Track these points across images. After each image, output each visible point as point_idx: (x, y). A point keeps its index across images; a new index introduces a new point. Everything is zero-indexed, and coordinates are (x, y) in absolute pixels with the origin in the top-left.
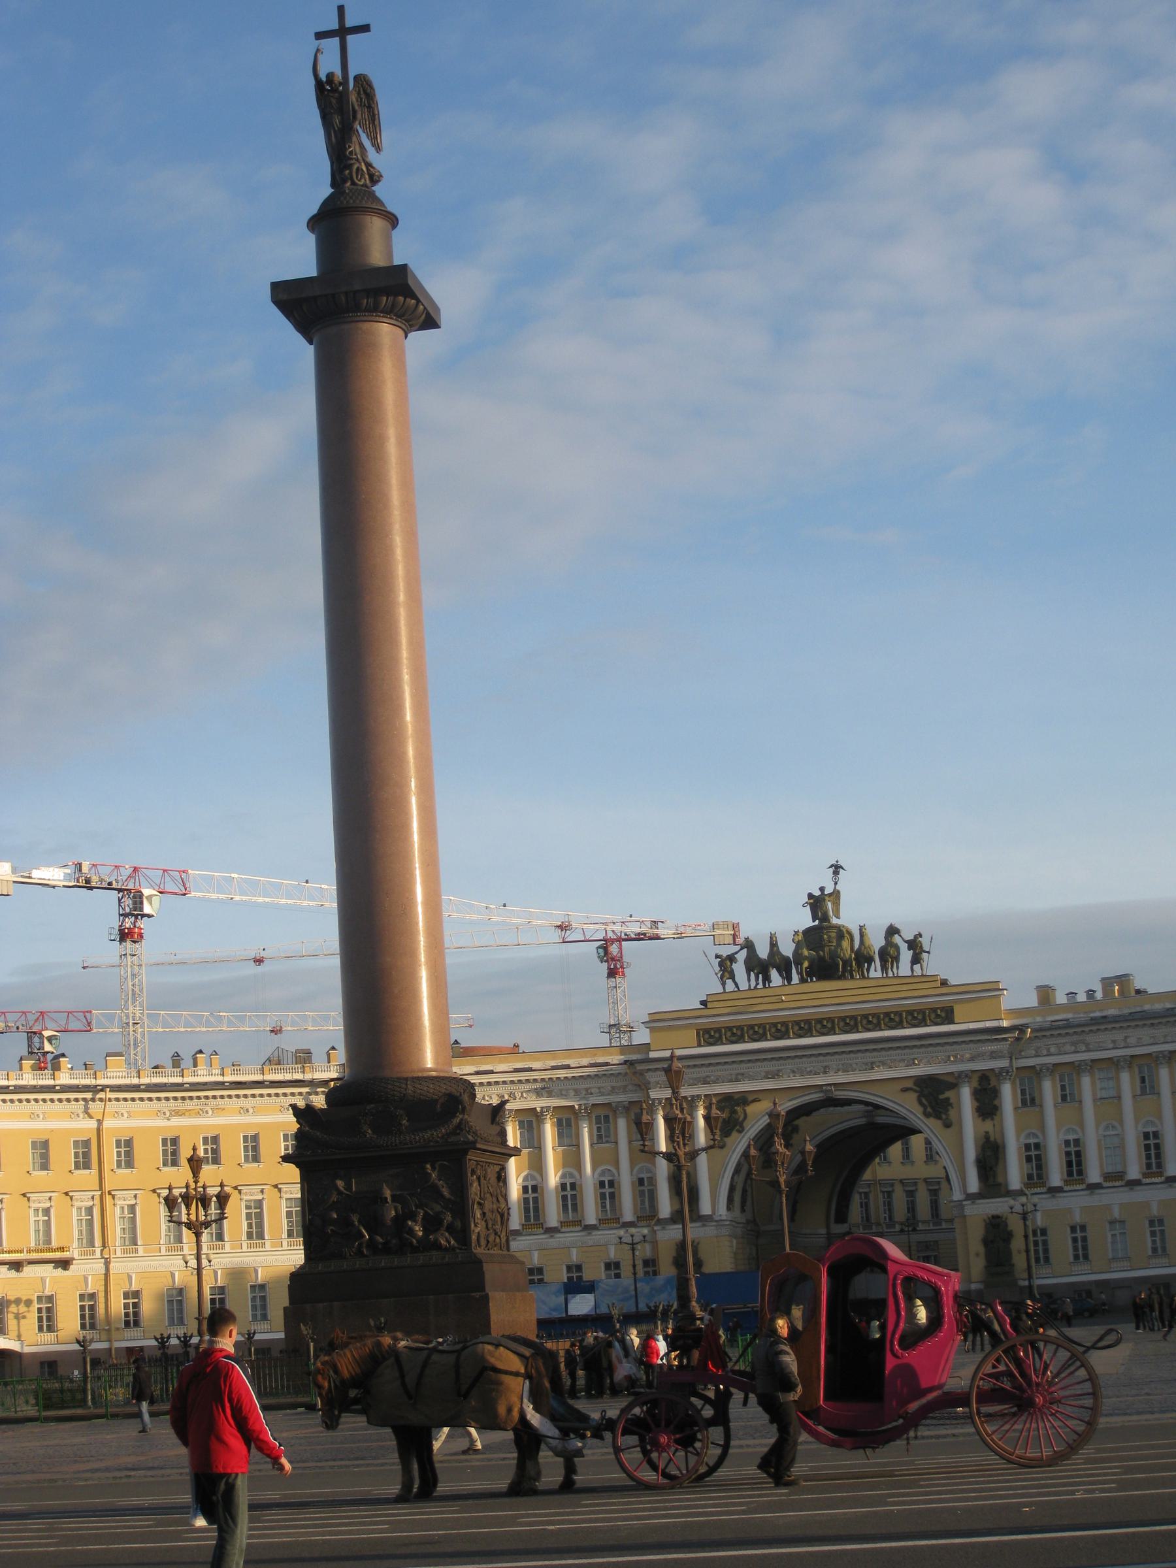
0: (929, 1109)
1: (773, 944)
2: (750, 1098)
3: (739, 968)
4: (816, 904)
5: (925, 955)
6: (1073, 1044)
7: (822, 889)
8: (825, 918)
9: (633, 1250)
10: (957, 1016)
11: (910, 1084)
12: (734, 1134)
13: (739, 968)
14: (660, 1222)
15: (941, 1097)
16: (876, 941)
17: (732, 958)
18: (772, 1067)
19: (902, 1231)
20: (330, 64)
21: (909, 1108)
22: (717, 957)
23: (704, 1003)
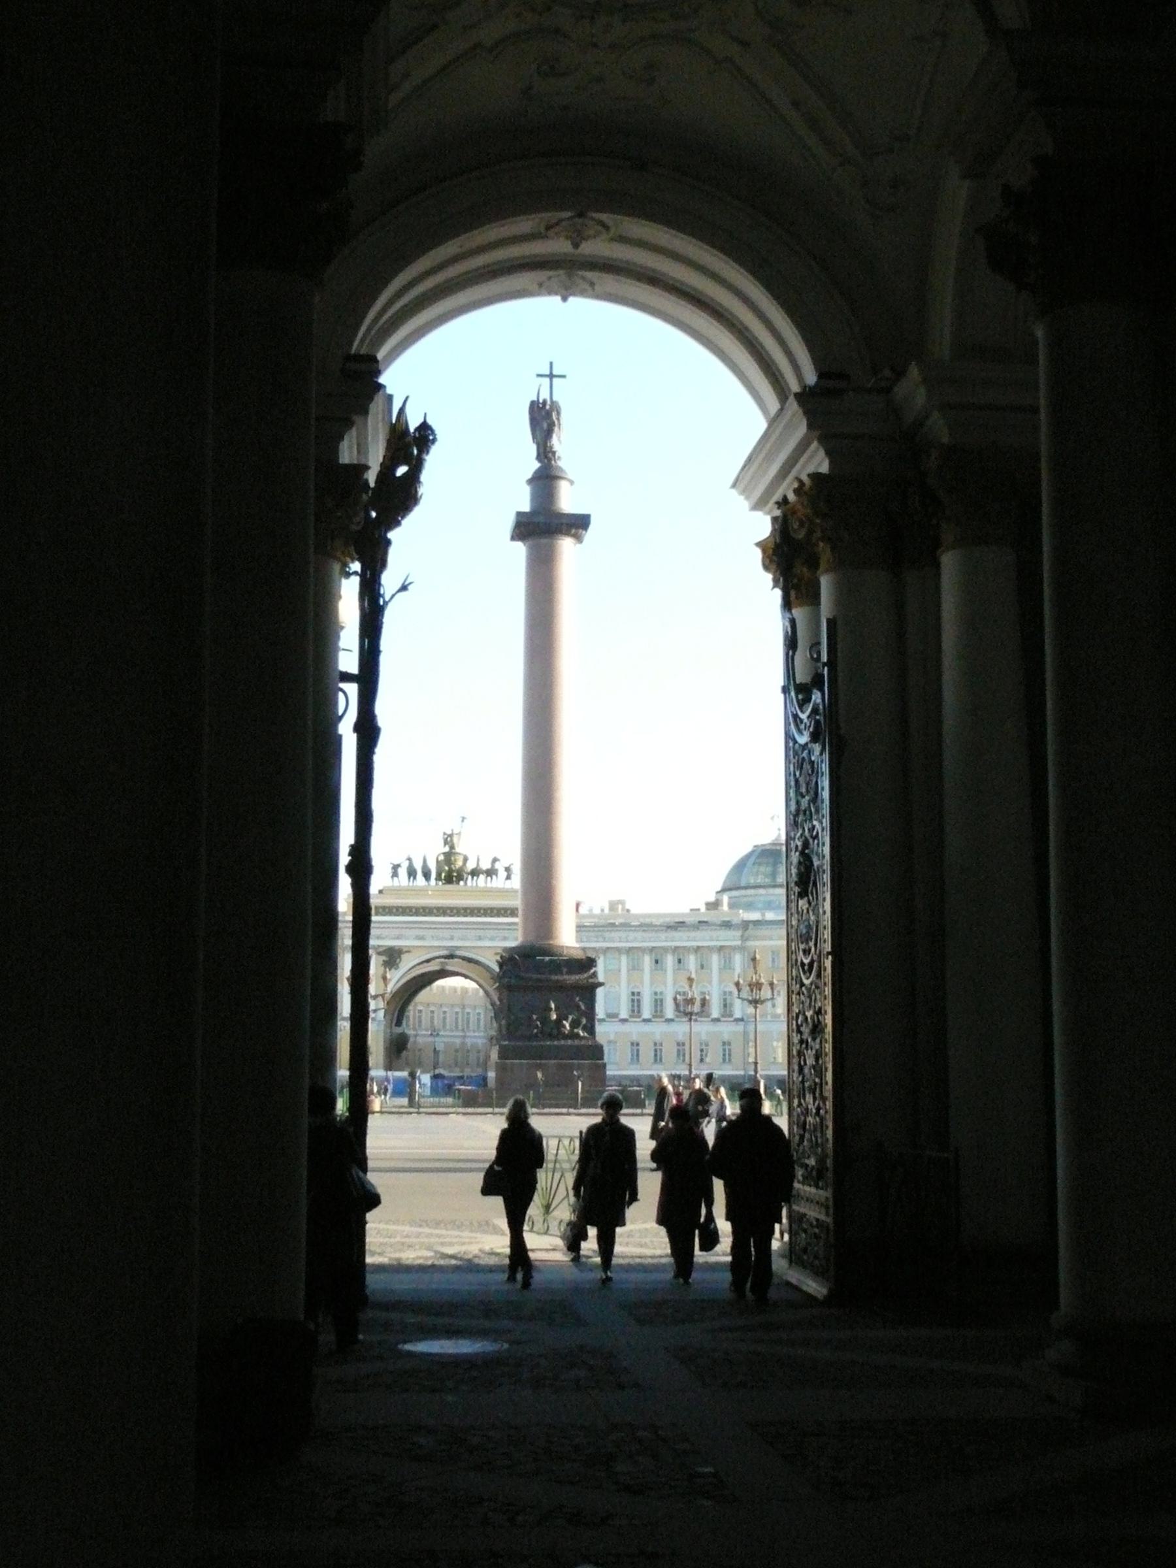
1: (425, 861)
3: (403, 872)
4: (448, 840)
6: (597, 937)
8: (452, 847)
13: (403, 872)
16: (485, 865)
17: (399, 866)
18: (421, 933)
20: (544, 395)
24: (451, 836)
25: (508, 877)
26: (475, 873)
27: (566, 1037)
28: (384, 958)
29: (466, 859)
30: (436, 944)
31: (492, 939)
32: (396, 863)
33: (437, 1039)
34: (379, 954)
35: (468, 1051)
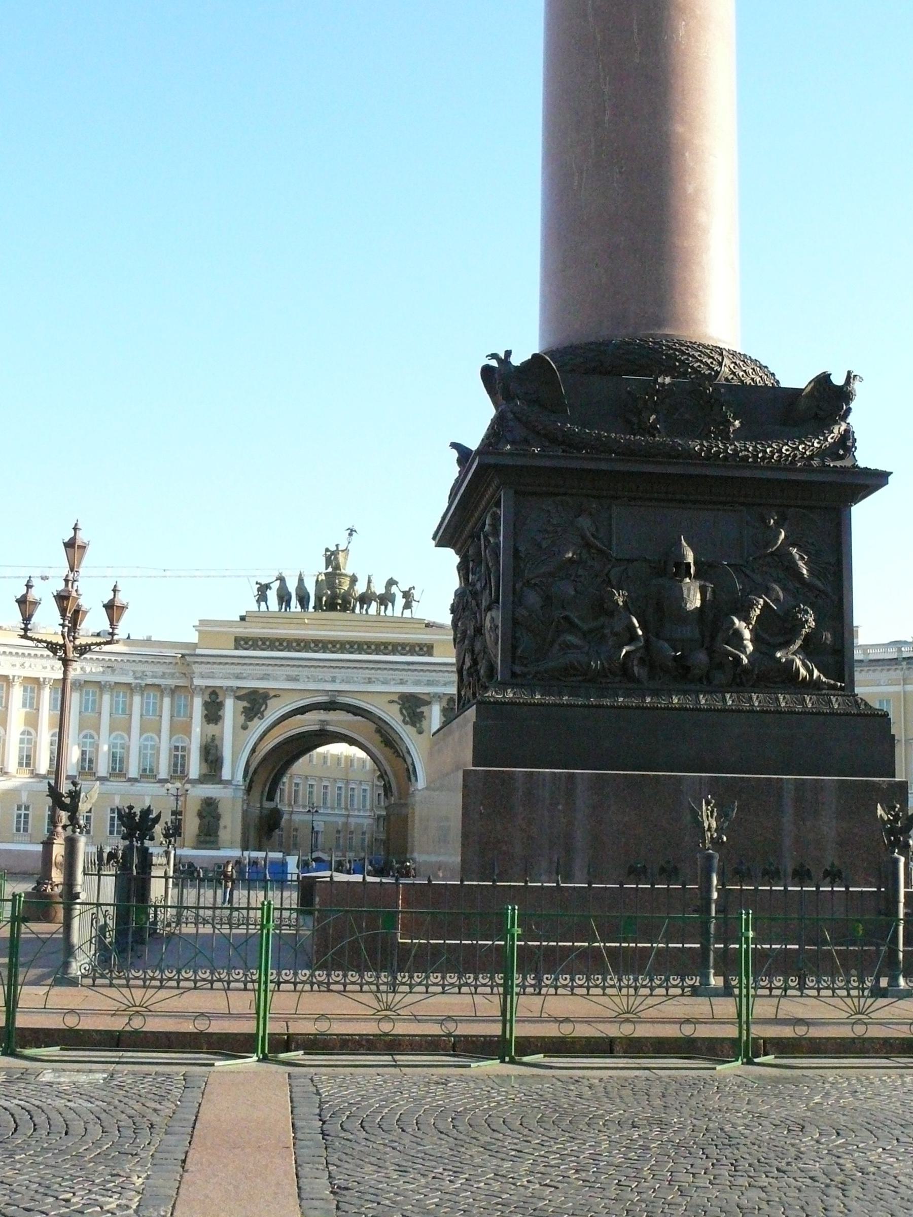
0: (407, 719)
1: (301, 580)
2: (272, 694)
3: (272, 595)
4: (332, 558)
5: (414, 603)
7: (337, 546)
8: (337, 567)
9: (177, 800)
10: (435, 651)
11: (395, 698)
12: (256, 719)
13: (272, 595)
14: (189, 781)
15: (418, 710)
16: (379, 589)
17: (267, 586)
19: (309, 811)
21: (393, 716)
22: (257, 583)
23: (243, 618)
24: (335, 553)
25: (408, 606)
26: (365, 599)
27: (741, 679)
28: (245, 704)
29: (354, 580)
30: (312, 686)
31: (385, 682)
32: (264, 581)
33: (315, 818)
34: (238, 698)
35: (351, 833)
